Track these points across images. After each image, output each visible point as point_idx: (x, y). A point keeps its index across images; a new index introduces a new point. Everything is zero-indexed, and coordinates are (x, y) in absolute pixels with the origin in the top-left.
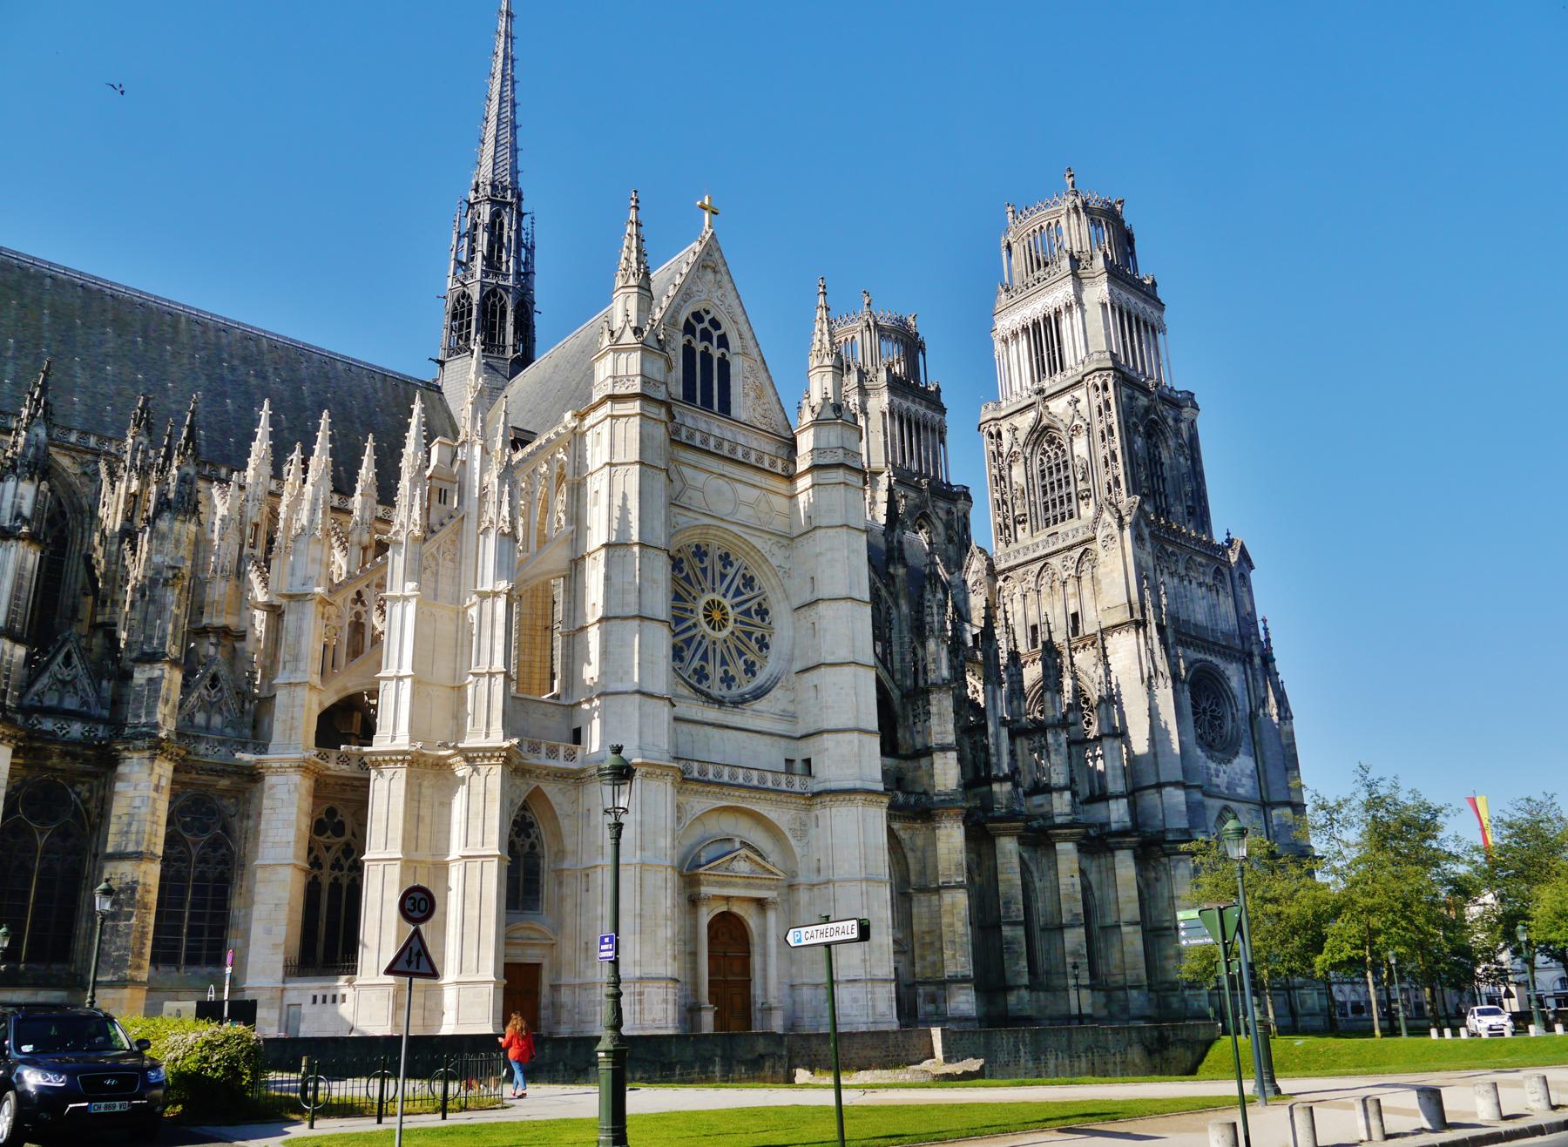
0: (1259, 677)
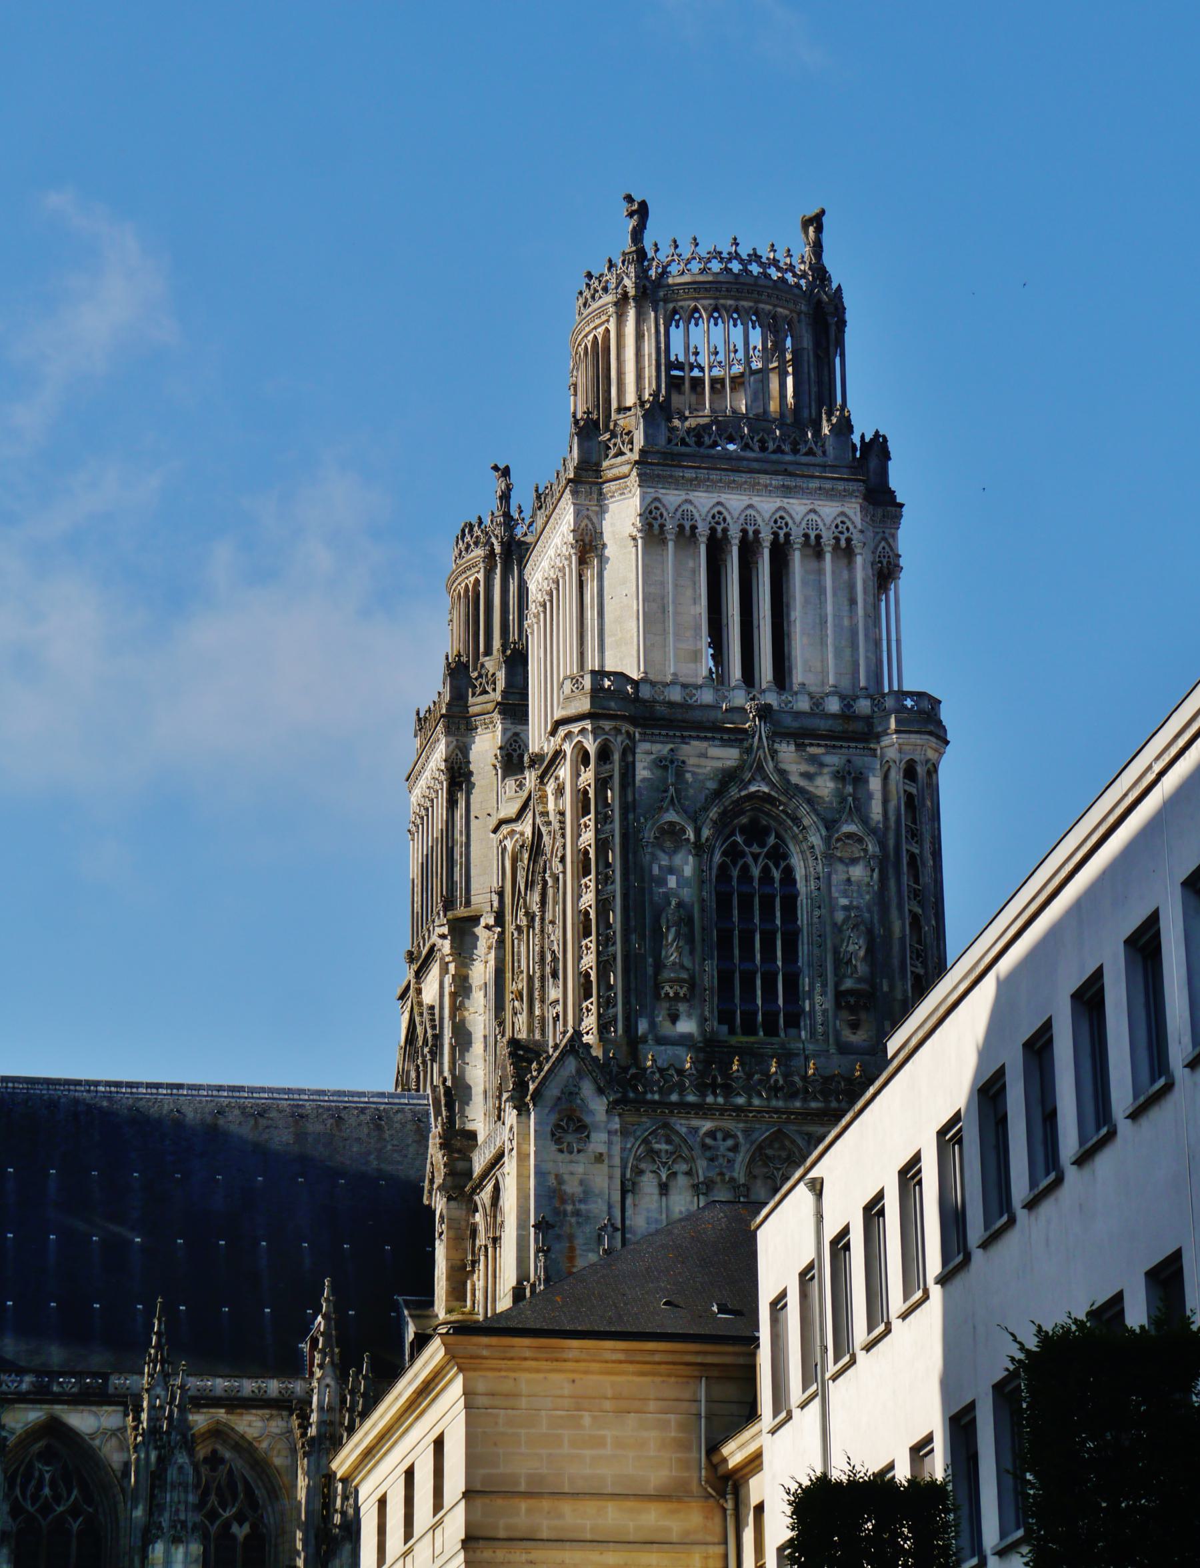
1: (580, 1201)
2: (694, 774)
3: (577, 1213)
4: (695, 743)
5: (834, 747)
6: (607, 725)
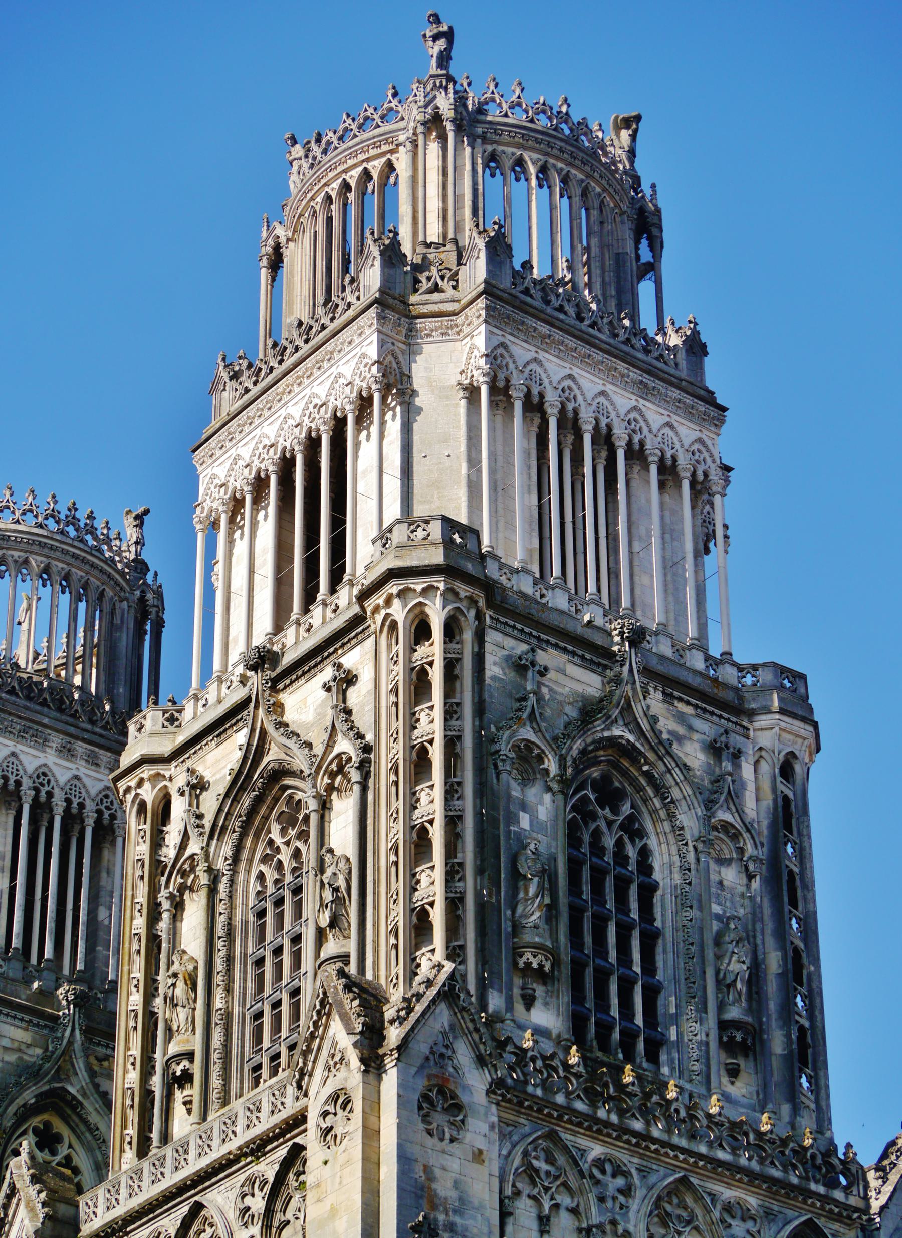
1: (455, 1212)
2: (551, 690)
4: (551, 650)
5: (705, 710)
6: (464, 590)
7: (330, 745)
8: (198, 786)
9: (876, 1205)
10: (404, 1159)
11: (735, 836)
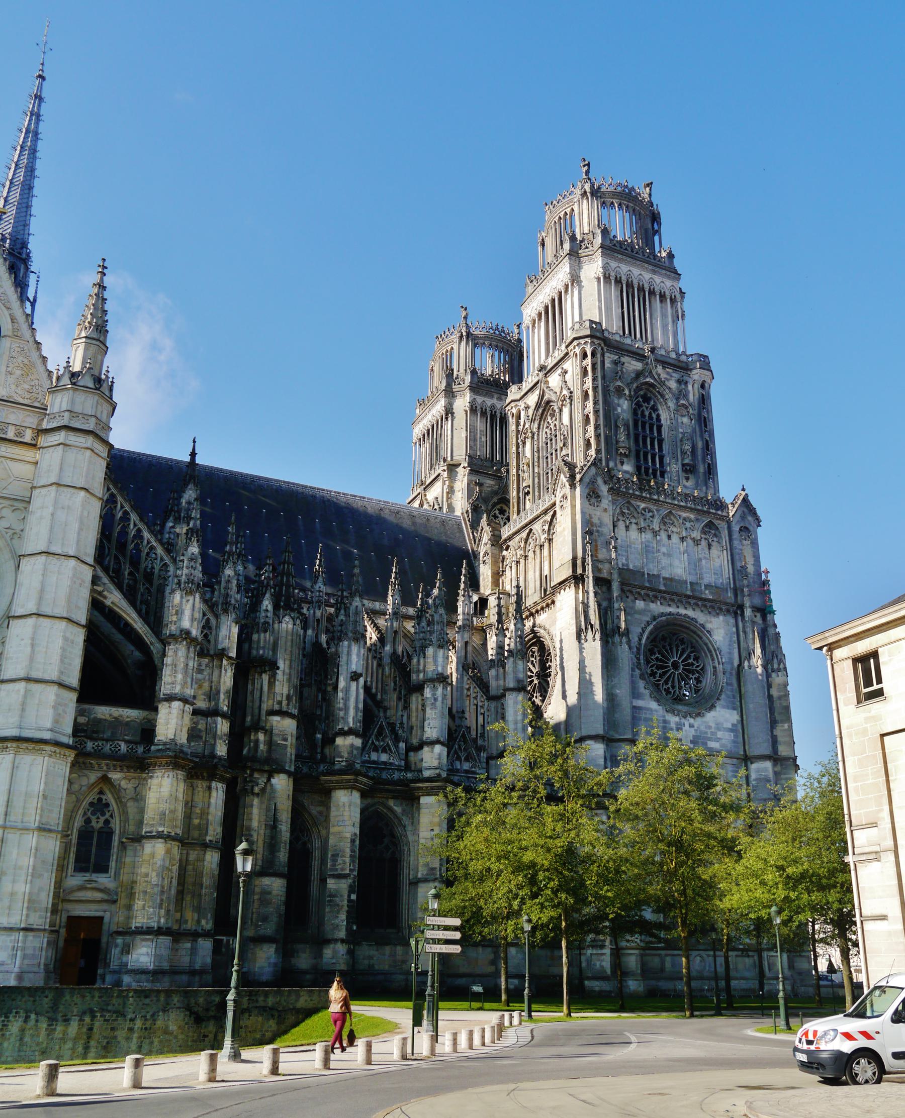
0: (749, 630)
3: (598, 531)
6: (596, 341)
7: (561, 392)
8: (527, 408)
9: (731, 514)
10: (583, 513)
11: (687, 408)
